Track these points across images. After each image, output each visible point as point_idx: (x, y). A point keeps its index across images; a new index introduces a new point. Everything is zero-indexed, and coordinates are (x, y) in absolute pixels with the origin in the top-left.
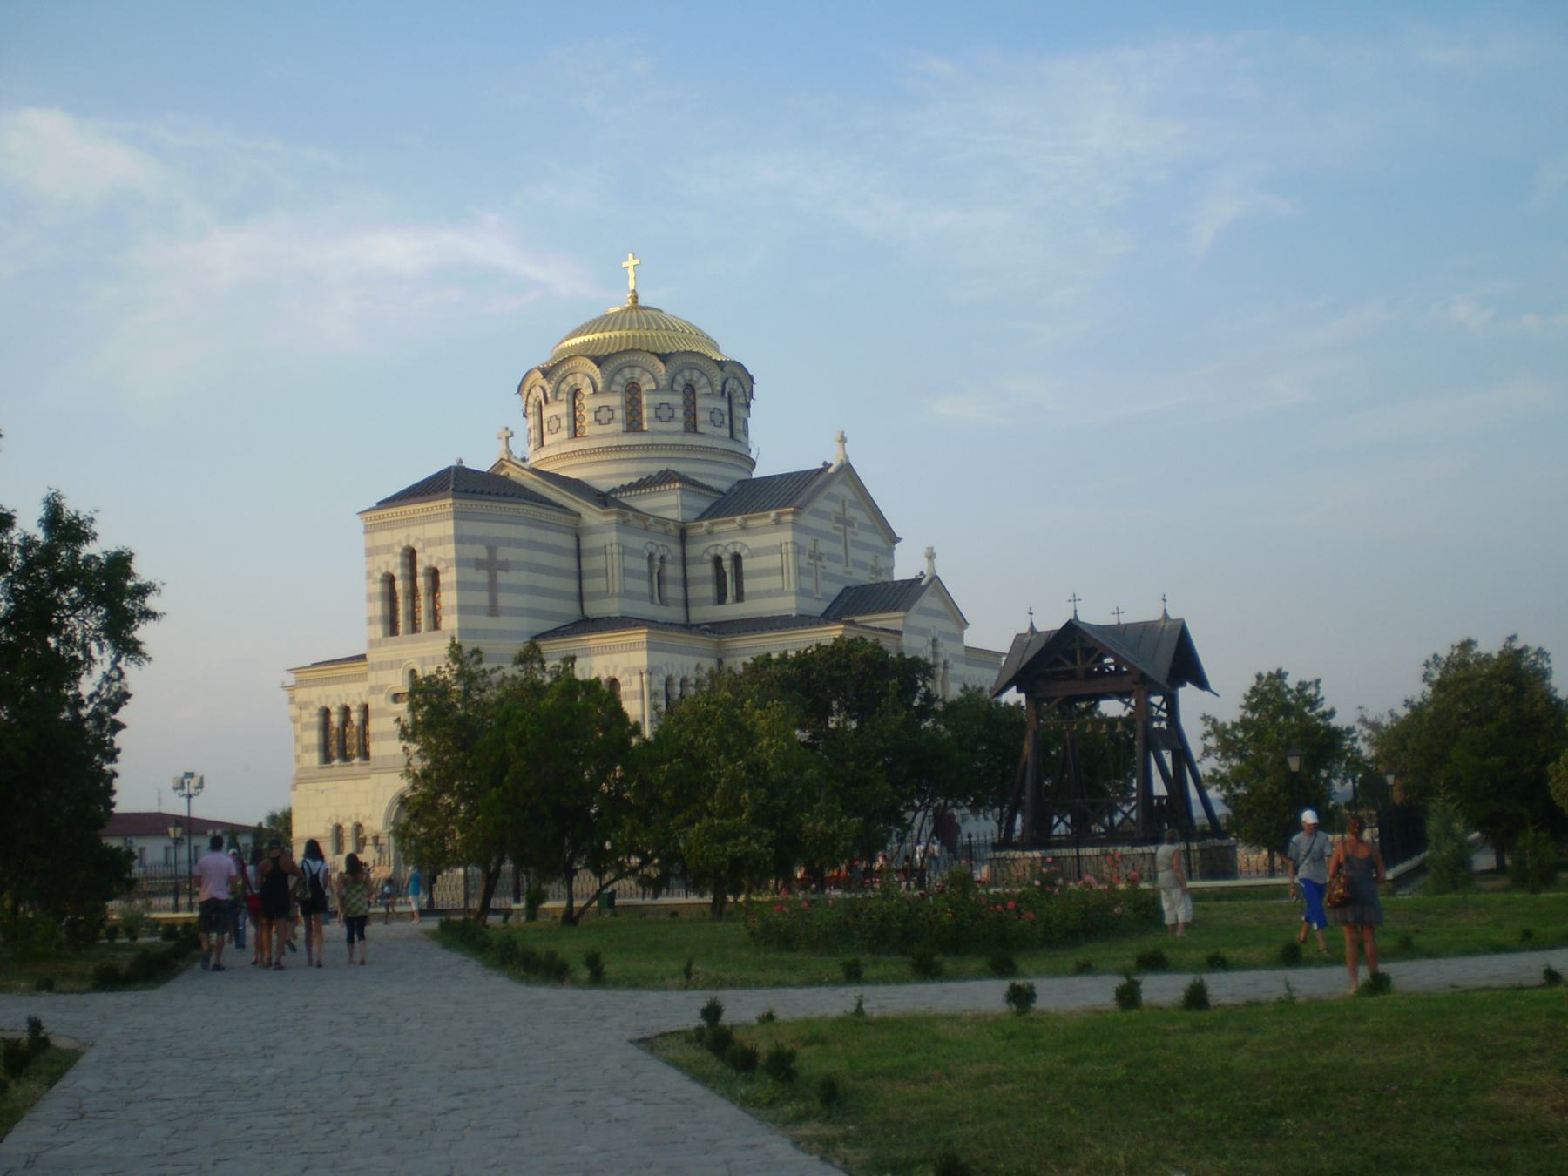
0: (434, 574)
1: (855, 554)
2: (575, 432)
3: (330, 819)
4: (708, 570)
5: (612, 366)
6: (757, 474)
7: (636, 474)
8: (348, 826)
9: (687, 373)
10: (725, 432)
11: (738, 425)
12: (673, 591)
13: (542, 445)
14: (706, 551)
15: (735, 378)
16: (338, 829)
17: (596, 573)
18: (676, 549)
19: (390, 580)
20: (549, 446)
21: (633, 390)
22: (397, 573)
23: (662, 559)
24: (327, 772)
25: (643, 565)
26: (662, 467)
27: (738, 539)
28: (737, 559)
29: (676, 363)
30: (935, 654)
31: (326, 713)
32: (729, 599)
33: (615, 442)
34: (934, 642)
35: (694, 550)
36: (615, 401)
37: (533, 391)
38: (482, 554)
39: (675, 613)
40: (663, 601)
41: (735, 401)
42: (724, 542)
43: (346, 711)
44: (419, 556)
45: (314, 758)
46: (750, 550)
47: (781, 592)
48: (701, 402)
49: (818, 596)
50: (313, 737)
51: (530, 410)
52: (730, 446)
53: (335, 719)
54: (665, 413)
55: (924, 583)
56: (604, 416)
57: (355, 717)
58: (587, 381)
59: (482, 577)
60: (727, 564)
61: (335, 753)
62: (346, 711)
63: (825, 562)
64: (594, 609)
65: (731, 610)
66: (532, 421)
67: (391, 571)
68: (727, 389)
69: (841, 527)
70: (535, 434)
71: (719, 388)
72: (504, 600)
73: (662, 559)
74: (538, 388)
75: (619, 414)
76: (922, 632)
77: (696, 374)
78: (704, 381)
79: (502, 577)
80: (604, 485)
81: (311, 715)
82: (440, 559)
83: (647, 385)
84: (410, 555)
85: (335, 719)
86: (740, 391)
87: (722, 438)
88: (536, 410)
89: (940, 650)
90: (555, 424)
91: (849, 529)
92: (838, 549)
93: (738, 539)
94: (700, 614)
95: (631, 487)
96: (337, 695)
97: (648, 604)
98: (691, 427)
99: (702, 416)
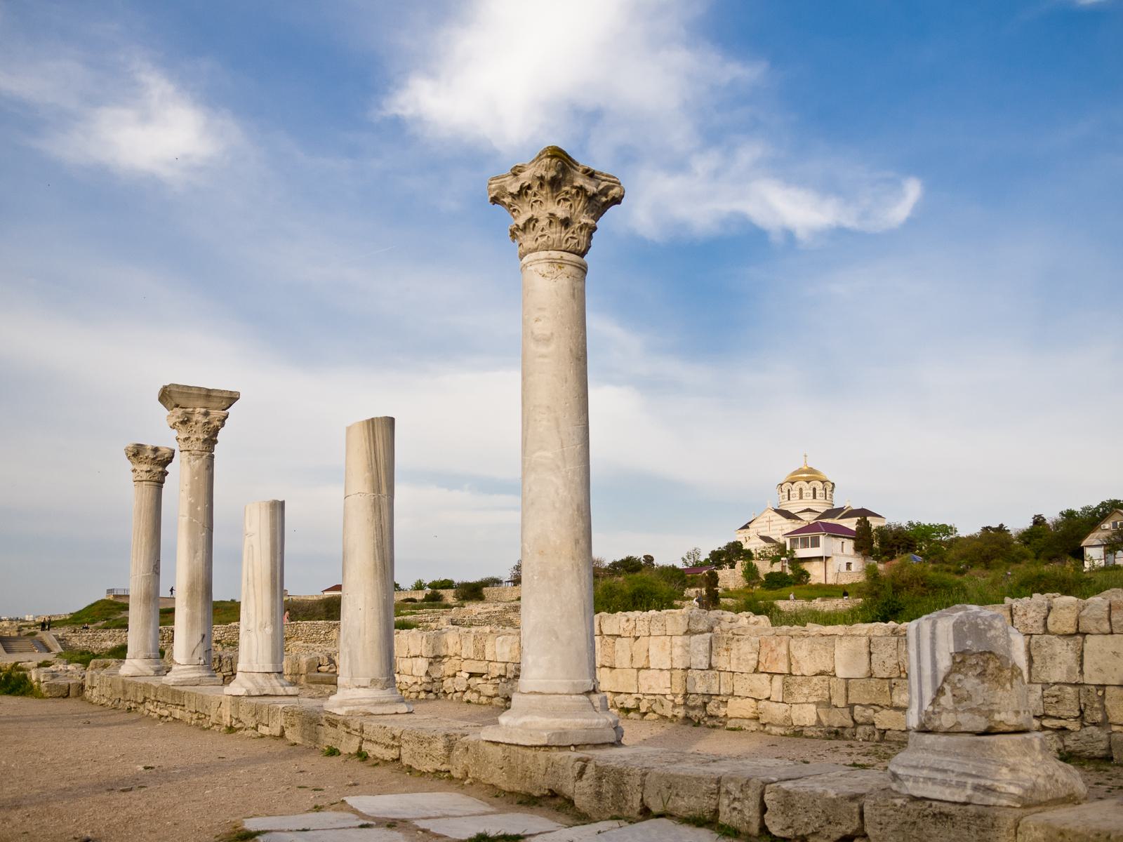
2: (789, 499)
5: (795, 484)
6: (834, 507)
10: (824, 498)
11: (828, 496)
21: (801, 490)
26: (807, 507)
29: (811, 483)
33: (795, 502)
36: (798, 492)
48: (817, 492)
52: (826, 501)
54: (808, 495)
71: (822, 488)
75: (798, 495)
80: (793, 512)
95: (798, 513)
99: (817, 495)
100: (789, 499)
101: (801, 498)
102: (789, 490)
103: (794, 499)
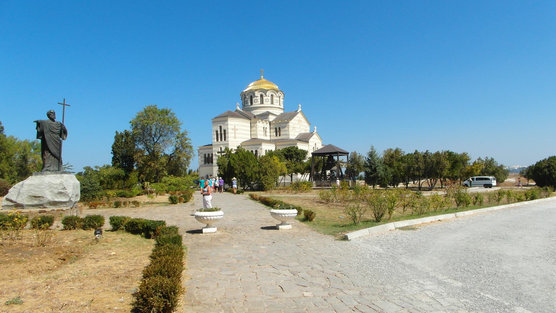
0: (225, 131)
1: (301, 127)
4: (274, 130)
7: (261, 112)
10: (279, 104)
12: (268, 134)
13: (244, 106)
14: (274, 126)
15: (281, 94)
16: (207, 176)
17: (254, 131)
18: (268, 126)
19: (217, 132)
20: (246, 106)
22: (219, 130)
23: (266, 128)
25: (262, 129)
28: (280, 128)
30: (315, 146)
31: (205, 155)
32: (278, 136)
33: (257, 106)
34: (315, 144)
35: (272, 126)
36: (259, 98)
38: (233, 127)
39: (268, 138)
40: (266, 136)
41: (280, 98)
43: (209, 154)
44: (222, 127)
45: (203, 163)
49: (294, 135)
50: (203, 159)
51: (242, 99)
53: (207, 156)
54: (267, 100)
55: (314, 133)
56: (256, 101)
57: (210, 156)
59: (233, 131)
60: (278, 129)
62: (209, 154)
63: (296, 129)
64: (253, 137)
65: (278, 138)
66: (243, 101)
68: (279, 96)
69: (299, 122)
70: (243, 103)
71: (278, 96)
72: (237, 135)
73: (266, 128)
76: (313, 142)
78: (274, 94)
79: (236, 131)
80: (256, 114)
83: (264, 94)
84: (221, 127)
85: (207, 156)
86: (281, 96)
87: (278, 105)
89: (316, 145)
90: (247, 102)
91: (301, 123)
92: (299, 126)
94: (273, 138)
96: (207, 152)
97: (263, 136)
98: (272, 103)
99: (274, 101)
100: (252, 103)
101: (262, 102)
102: (251, 98)
103: (257, 103)
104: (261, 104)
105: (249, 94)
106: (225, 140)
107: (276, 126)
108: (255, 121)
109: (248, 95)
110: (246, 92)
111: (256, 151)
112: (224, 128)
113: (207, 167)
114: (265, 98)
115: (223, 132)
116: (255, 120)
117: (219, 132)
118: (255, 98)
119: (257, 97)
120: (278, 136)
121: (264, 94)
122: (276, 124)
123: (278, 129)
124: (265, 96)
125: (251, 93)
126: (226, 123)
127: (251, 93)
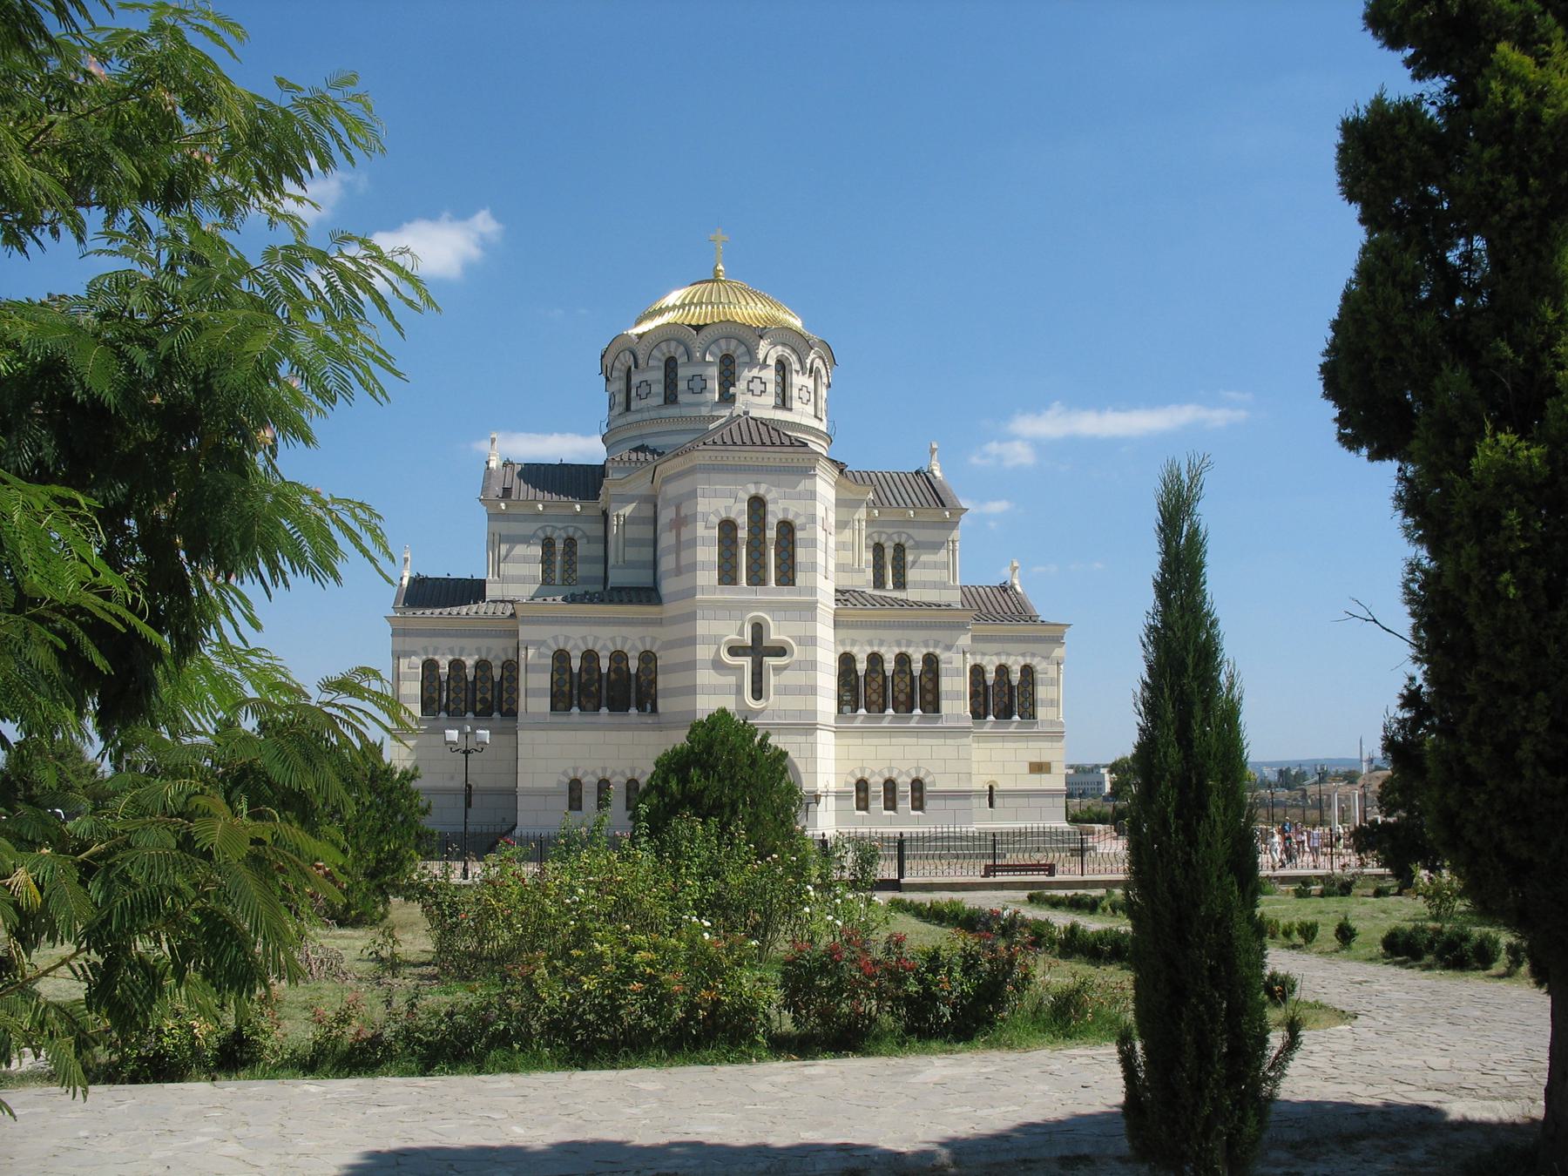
0: (787, 529)
3: (565, 773)
4: (868, 556)
8: (590, 782)
9: (817, 360)
22: (743, 521)
24: (563, 719)
27: (905, 530)
28: (900, 549)
36: (770, 375)
37: (663, 345)
42: (890, 531)
44: (770, 507)
46: (916, 542)
47: (943, 586)
53: (576, 664)
56: (757, 386)
58: (742, 349)
60: (889, 554)
61: (576, 702)
67: (732, 516)
70: (658, 388)
74: (673, 344)
75: (771, 388)
77: (821, 363)
78: (823, 372)
81: (541, 655)
82: (797, 515)
84: (757, 505)
85: (576, 664)
88: (662, 365)
93: (901, 530)
99: (822, 404)
101: (783, 402)
104: (776, 407)
105: (716, 341)
106: (787, 575)
107: (880, 533)
108: (853, 497)
109: (713, 347)
110: (698, 328)
111: (931, 661)
112: (785, 510)
113: (580, 734)
114: (799, 380)
115: (771, 534)
116: (851, 492)
117: (743, 534)
118: (755, 372)
119: (764, 365)
120: (890, 585)
121: (793, 358)
122: (884, 524)
123: (889, 554)
124: (797, 372)
125: (734, 343)
126: (804, 485)
127: (734, 343)
